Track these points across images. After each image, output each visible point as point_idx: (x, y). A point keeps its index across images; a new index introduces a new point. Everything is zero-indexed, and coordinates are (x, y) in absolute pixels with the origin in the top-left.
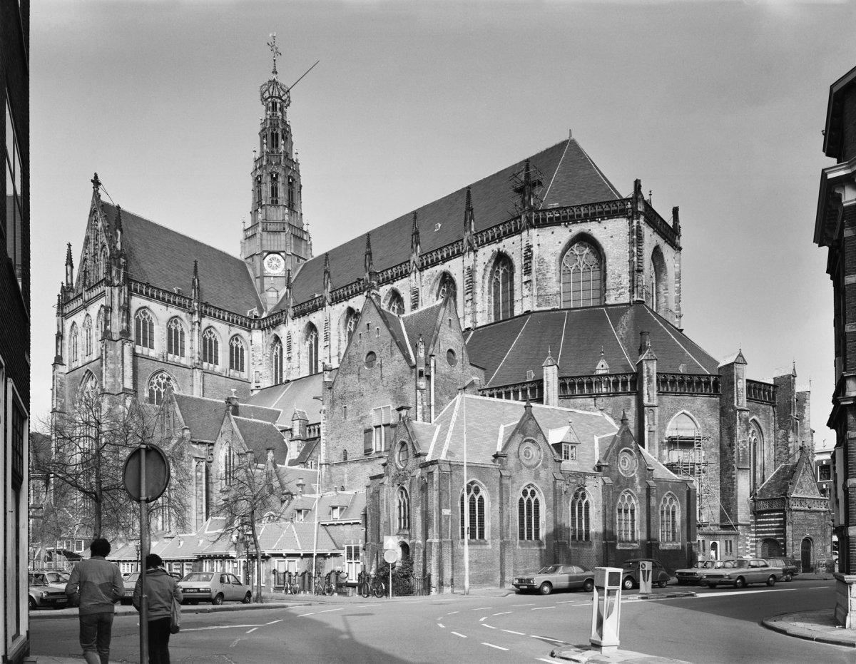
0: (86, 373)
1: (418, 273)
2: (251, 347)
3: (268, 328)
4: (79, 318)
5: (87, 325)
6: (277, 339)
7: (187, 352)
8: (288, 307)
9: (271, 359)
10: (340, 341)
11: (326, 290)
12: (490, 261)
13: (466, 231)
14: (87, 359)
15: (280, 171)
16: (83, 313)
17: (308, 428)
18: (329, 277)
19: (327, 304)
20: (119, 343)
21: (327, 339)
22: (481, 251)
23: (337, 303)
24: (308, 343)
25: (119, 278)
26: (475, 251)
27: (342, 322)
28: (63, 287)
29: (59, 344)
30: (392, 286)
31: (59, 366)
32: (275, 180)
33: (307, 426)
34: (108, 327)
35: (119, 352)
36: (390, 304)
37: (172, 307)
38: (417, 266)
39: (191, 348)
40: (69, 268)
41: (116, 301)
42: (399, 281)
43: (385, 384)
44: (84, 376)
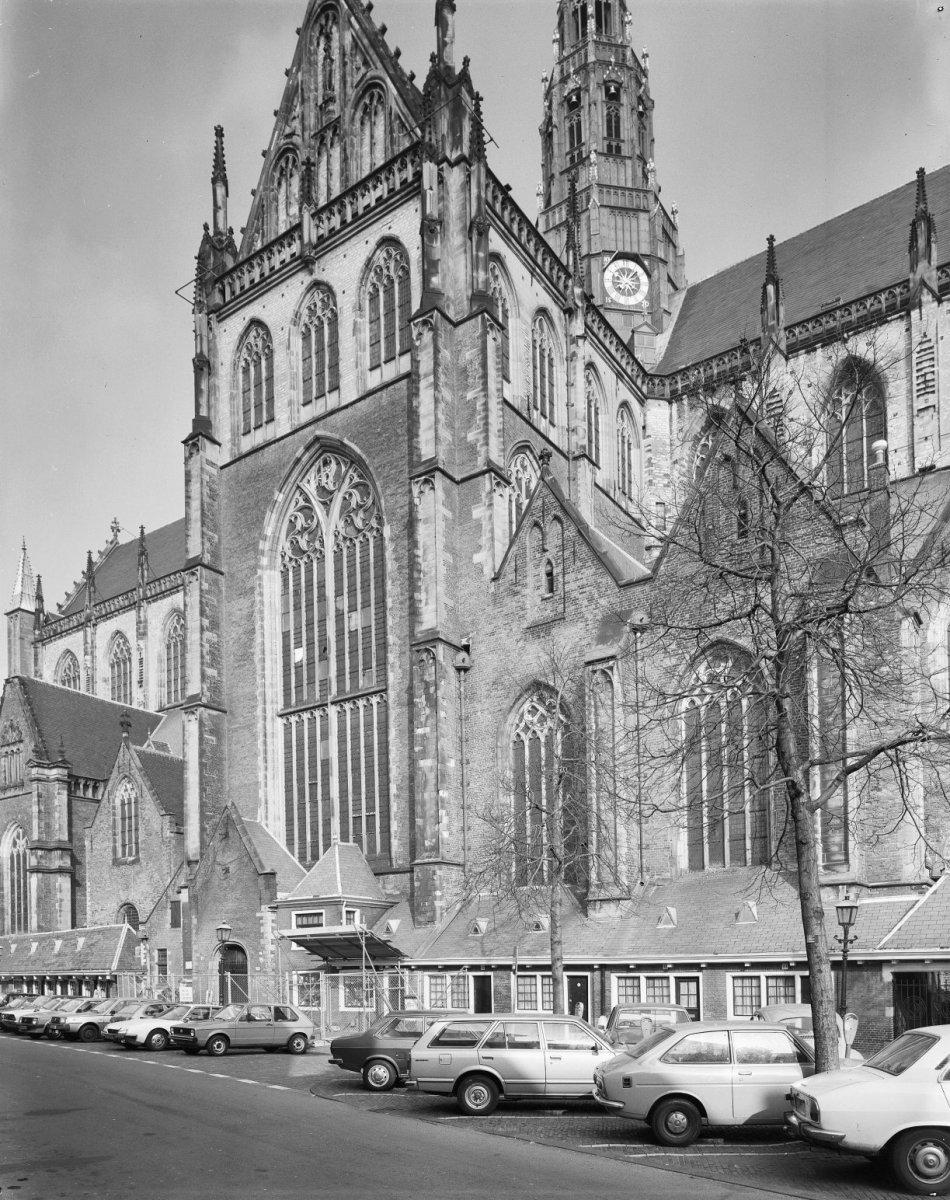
0: (307, 449)
2: (644, 442)
4: (280, 306)
5: (305, 319)
11: (922, 265)
14: (307, 413)
15: (624, 78)
16: (299, 282)
19: (926, 297)
20: (474, 327)
25: (457, 143)
28: (207, 239)
29: (204, 386)
31: (208, 443)
32: (613, 98)
34: (435, 280)
35: (469, 354)
39: (569, 405)
40: (220, 191)
41: (454, 208)
44: (298, 460)
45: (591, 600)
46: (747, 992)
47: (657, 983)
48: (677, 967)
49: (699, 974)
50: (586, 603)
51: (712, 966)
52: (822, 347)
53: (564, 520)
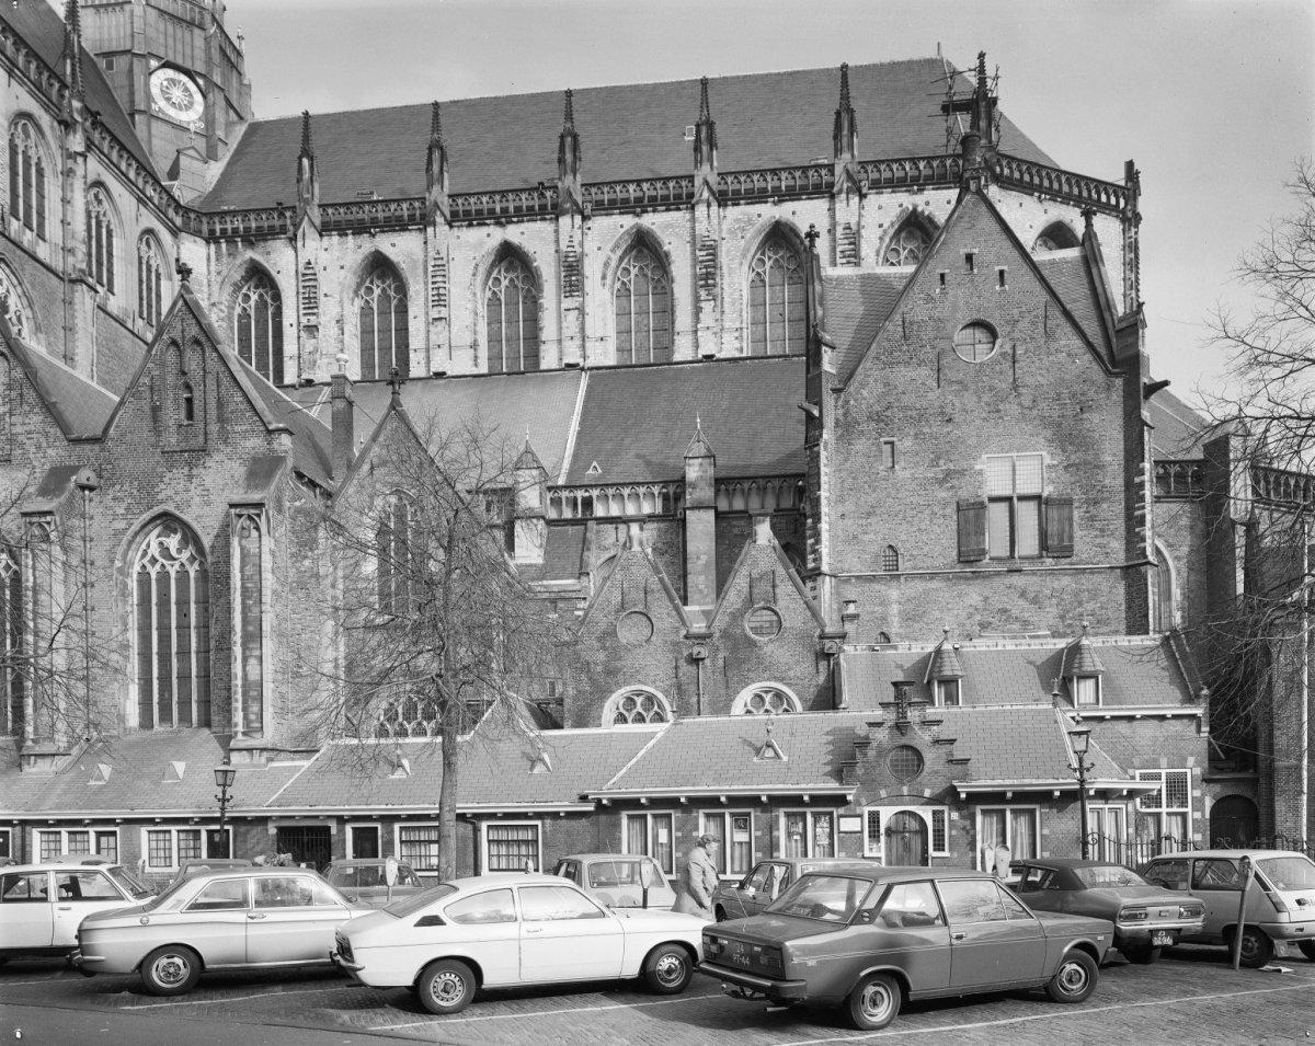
1: (714, 207)
3: (231, 241)
6: (259, 276)
7: (53, 228)
8: (307, 202)
9: (230, 318)
10: (476, 314)
12: (892, 224)
13: (838, 151)
17: (549, 495)
18: (443, 158)
21: (440, 300)
22: (873, 200)
23: (470, 225)
24: (358, 303)
26: (862, 196)
27: (482, 270)
30: (637, 220)
33: (549, 489)
36: (621, 259)
37: (22, 84)
38: (710, 189)
42: (657, 215)
43: (1027, 402)
45: (39, 447)
46: (161, 845)
47: (79, 837)
48: (95, 822)
49: (117, 829)
50: (33, 449)
51: (127, 821)
52: (353, 234)
53: (11, 360)
